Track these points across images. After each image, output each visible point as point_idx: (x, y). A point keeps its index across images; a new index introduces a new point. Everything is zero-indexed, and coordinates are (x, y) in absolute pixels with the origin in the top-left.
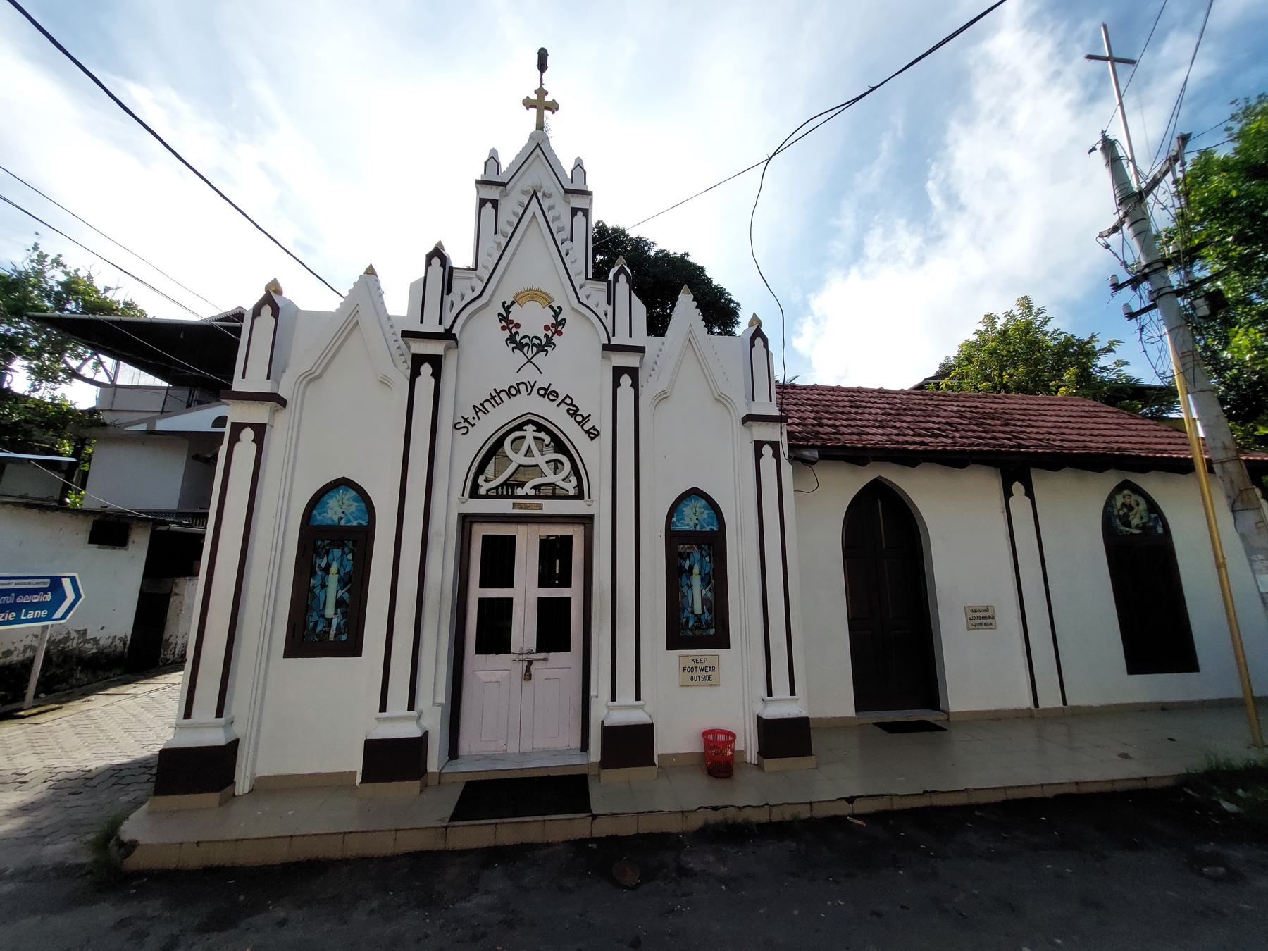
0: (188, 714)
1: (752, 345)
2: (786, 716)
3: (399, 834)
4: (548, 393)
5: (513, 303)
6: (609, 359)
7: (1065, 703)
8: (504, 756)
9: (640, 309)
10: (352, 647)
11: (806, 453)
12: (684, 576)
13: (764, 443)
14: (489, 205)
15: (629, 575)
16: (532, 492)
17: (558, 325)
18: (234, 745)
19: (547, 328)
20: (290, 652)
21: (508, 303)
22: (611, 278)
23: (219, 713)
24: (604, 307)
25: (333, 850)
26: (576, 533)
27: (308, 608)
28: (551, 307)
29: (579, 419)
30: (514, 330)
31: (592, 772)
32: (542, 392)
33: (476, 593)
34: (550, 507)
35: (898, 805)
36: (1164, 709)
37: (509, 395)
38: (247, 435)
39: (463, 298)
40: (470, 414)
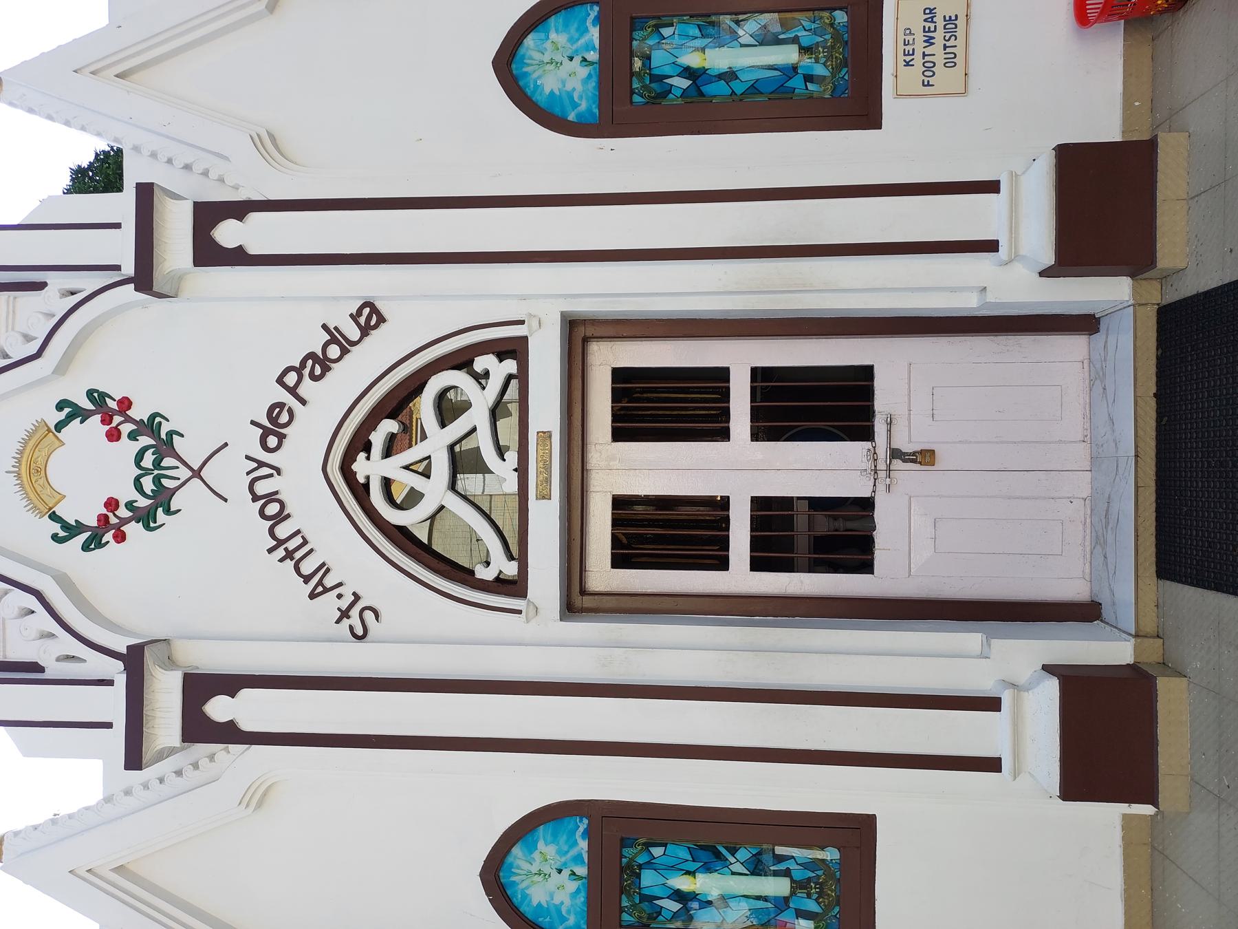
4: (274, 427)
5: (54, 517)
6: (179, 278)
10: (856, 834)
12: (710, 89)
16: (512, 457)
17: (106, 409)
19: (114, 435)
21: (56, 528)
24: (52, 301)
28: (60, 426)
29: (334, 351)
30: (123, 512)
31: (1156, 295)
32: (272, 441)
33: (740, 577)
34: (546, 411)
39: (51, 635)
40: (329, 604)
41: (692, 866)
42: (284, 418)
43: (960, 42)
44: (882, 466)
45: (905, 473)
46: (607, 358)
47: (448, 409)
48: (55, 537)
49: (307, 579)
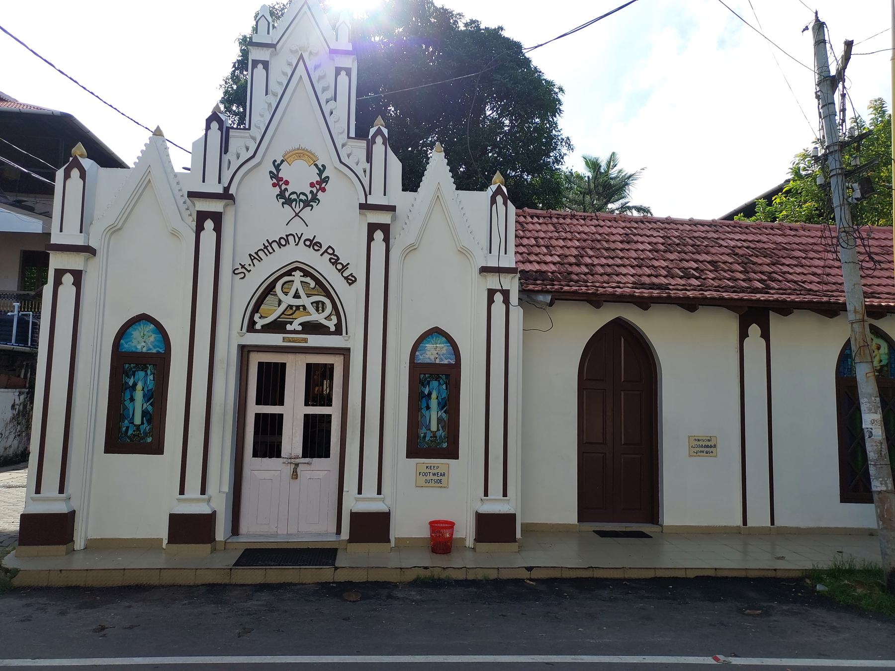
0: (38, 491)
2: (497, 512)
3: (198, 572)
4: (313, 244)
5: (282, 161)
7: (772, 523)
8: (276, 535)
9: (396, 167)
10: (157, 448)
11: (541, 298)
12: (424, 401)
13: (495, 291)
14: (260, 66)
16: (300, 328)
17: (322, 183)
18: (73, 513)
19: (312, 185)
20: (108, 450)
21: (278, 162)
23: (61, 491)
25: (154, 580)
27: (122, 418)
28: (316, 165)
30: (283, 187)
32: (308, 243)
33: (253, 409)
35: (566, 575)
36: (871, 535)
37: (280, 245)
38: (68, 279)
41: (146, 389)
42: (316, 248)
43: (433, 484)
44: (293, 460)
45: (289, 469)
46: (337, 362)
47: (319, 306)
48: (275, 161)
49: (257, 253)
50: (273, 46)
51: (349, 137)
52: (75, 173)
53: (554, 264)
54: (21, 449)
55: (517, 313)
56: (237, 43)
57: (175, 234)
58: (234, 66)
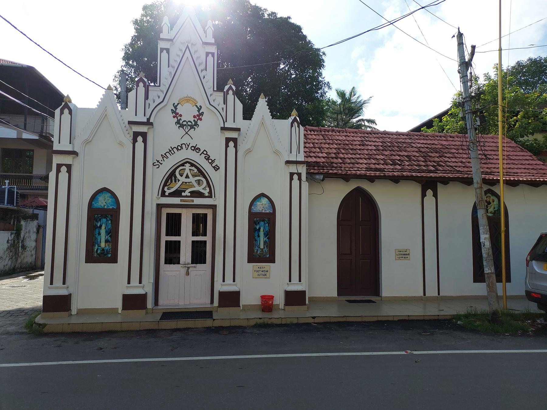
0: (51, 283)
1: (292, 126)
4: (196, 149)
5: (178, 104)
7: (439, 294)
9: (240, 106)
10: (114, 260)
11: (317, 177)
12: (256, 232)
13: (294, 173)
14: (165, 51)
15: (232, 231)
16: (189, 194)
19: (194, 117)
20: (87, 261)
21: (176, 104)
22: (225, 90)
23: (64, 283)
25: (119, 329)
26: (209, 212)
28: (196, 106)
30: (179, 118)
32: (193, 148)
33: (164, 238)
35: (333, 320)
37: (178, 149)
38: (64, 169)
40: (160, 158)
41: (107, 228)
42: (197, 151)
45: (184, 271)
46: (209, 213)
47: (199, 182)
48: (174, 104)
50: (171, 40)
51: (214, 91)
52: (66, 111)
53: (324, 158)
54: (13, 266)
55: (305, 185)
56: (132, 23)
57: (121, 144)
58: (132, 38)
